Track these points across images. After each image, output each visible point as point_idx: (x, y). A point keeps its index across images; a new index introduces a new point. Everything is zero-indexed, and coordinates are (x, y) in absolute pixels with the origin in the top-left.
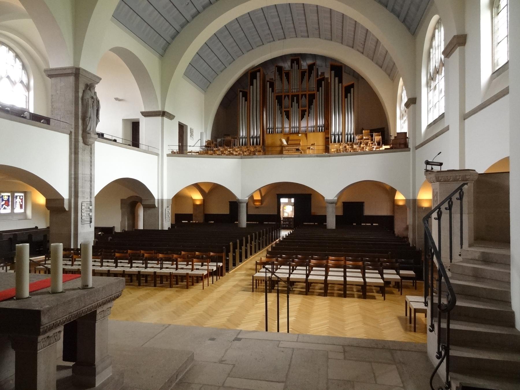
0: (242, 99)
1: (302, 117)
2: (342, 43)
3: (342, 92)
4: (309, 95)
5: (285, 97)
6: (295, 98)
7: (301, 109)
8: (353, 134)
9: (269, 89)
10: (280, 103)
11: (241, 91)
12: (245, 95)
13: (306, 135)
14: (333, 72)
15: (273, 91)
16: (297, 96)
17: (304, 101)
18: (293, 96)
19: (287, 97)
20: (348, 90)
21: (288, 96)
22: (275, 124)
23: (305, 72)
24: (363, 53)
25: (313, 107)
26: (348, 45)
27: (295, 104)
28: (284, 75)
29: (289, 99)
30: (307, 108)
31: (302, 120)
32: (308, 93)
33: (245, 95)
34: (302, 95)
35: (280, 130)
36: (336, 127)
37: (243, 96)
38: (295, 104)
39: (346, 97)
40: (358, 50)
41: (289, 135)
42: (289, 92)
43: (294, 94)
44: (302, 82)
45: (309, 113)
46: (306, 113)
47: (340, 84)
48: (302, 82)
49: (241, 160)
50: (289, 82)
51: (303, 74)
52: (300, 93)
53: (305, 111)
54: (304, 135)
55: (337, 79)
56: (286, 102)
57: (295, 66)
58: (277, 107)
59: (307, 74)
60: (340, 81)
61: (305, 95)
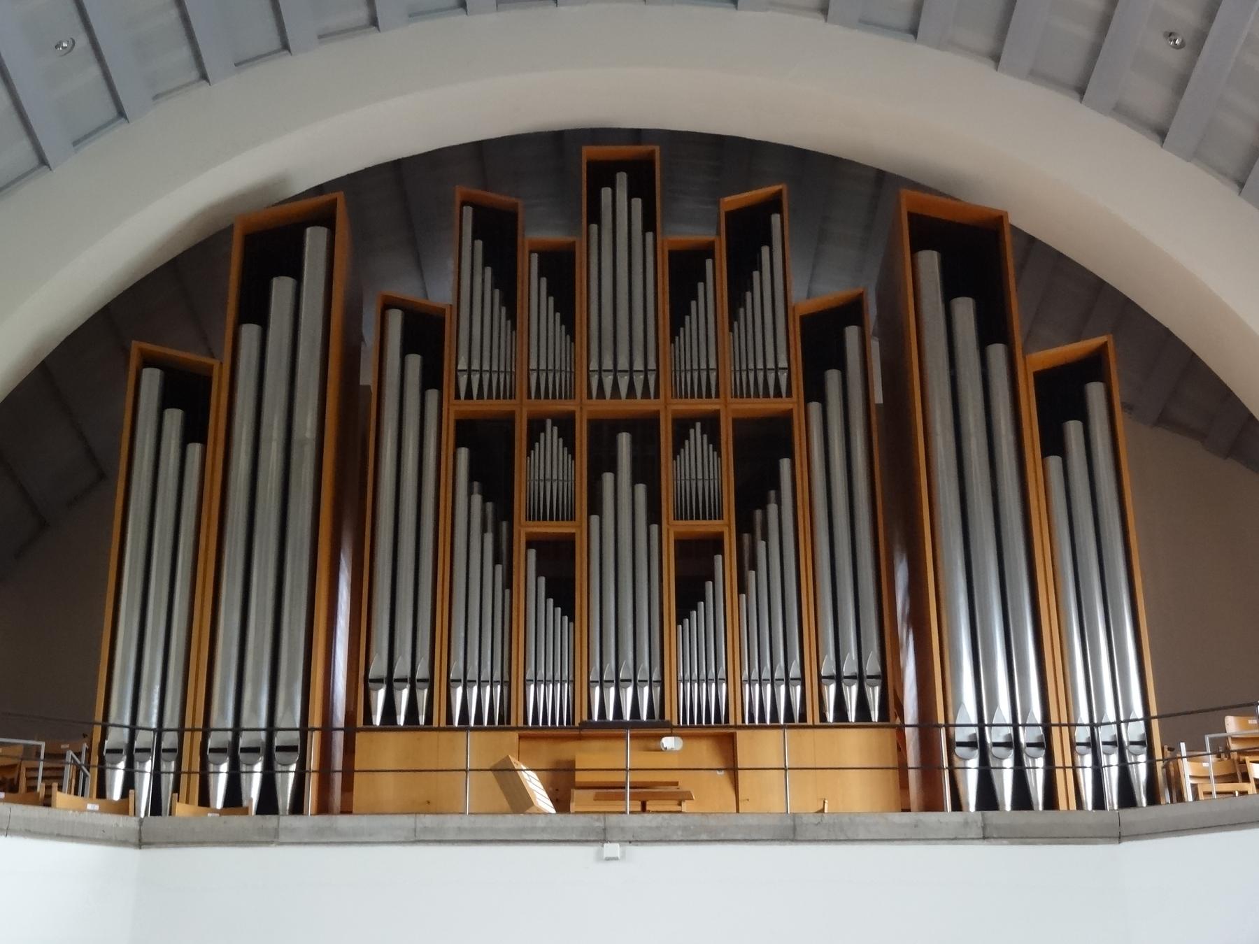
0: (154, 430)
1: (689, 597)
2: (996, 58)
3: (1011, 412)
4: (737, 423)
5: (536, 428)
6: (624, 440)
7: (673, 528)
8: (1147, 742)
9: (399, 371)
10: (494, 478)
11: (149, 361)
12: (189, 394)
13: (727, 744)
14: (930, 261)
15: (432, 378)
16: (645, 429)
17: (703, 468)
18: (604, 433)
19: (551, 434)
20: (1060, 396)
21: (566, 425)
22: (440, 646)
23: (707, 251)
24: (1161, 134)
25: (779, 515)
26: (1036, 75)
27: (621, 486)
28: (529, 269)
29: (570, 444)
30: (726, 526)
31: (683, 613)
32: (730, 408)
33: (189, 394)
34: (682, 427)
35: (490, 695)
36: (985, 694)
37: (166, 402)
38: (621, 486)
39: (1054, 444)
40: (1121, 112)
41: (568, 750)
42: (570, 395)
43: (607, 407)
44: (677, 324)
45: (746, 562)
46: (725, 565)
47: (997, 352)
48: (677, 324)
49: (131, 856)
50: (569, 322)
51: (685, 270)
52: (668, 407)
53: (716, 544)
54: (705, 753)
55: (965, 309)
56: (546, 467)
57: (618, 200)
58: (469, 506)
59: (716, 272)
60: (993, 328)
61: (711, 424)
